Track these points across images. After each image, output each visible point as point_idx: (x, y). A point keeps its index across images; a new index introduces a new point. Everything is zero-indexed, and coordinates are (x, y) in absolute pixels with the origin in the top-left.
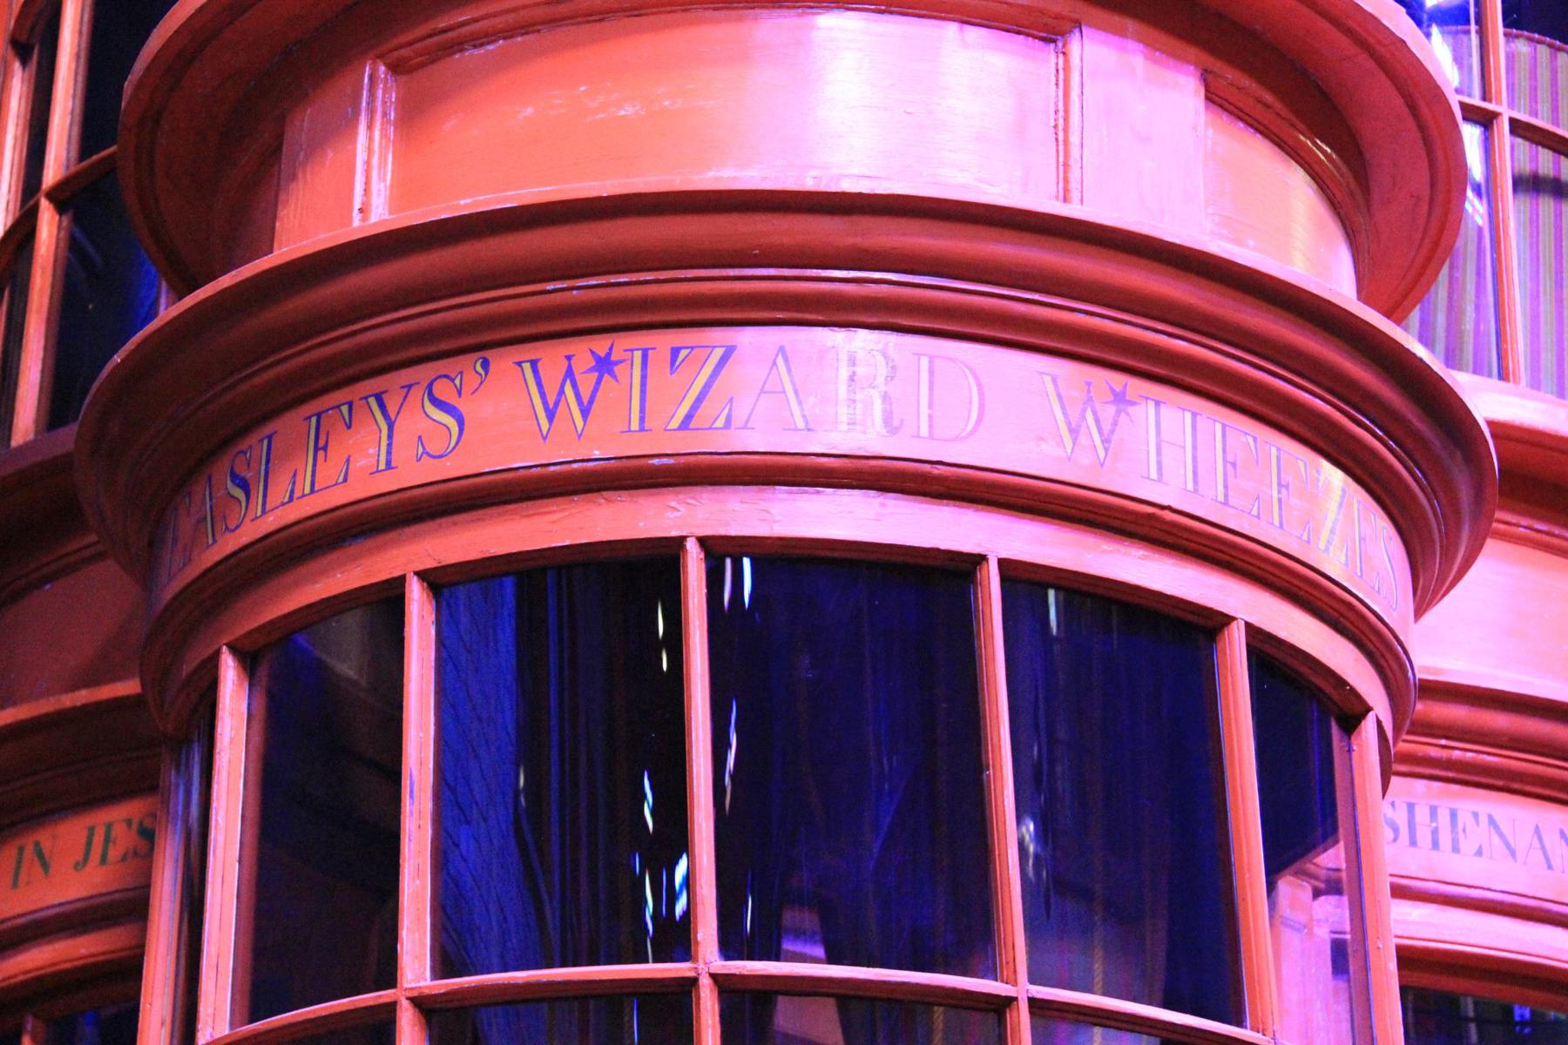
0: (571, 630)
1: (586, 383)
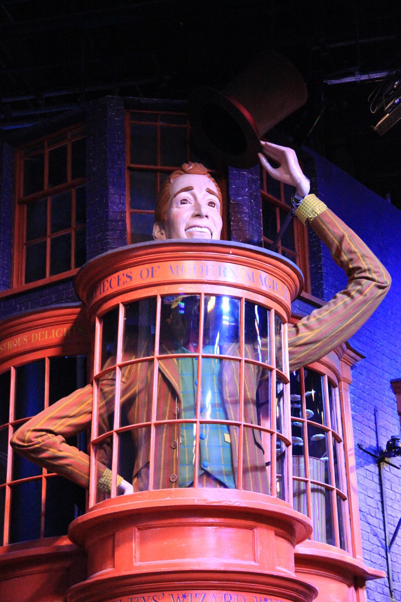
1: (182, 599)
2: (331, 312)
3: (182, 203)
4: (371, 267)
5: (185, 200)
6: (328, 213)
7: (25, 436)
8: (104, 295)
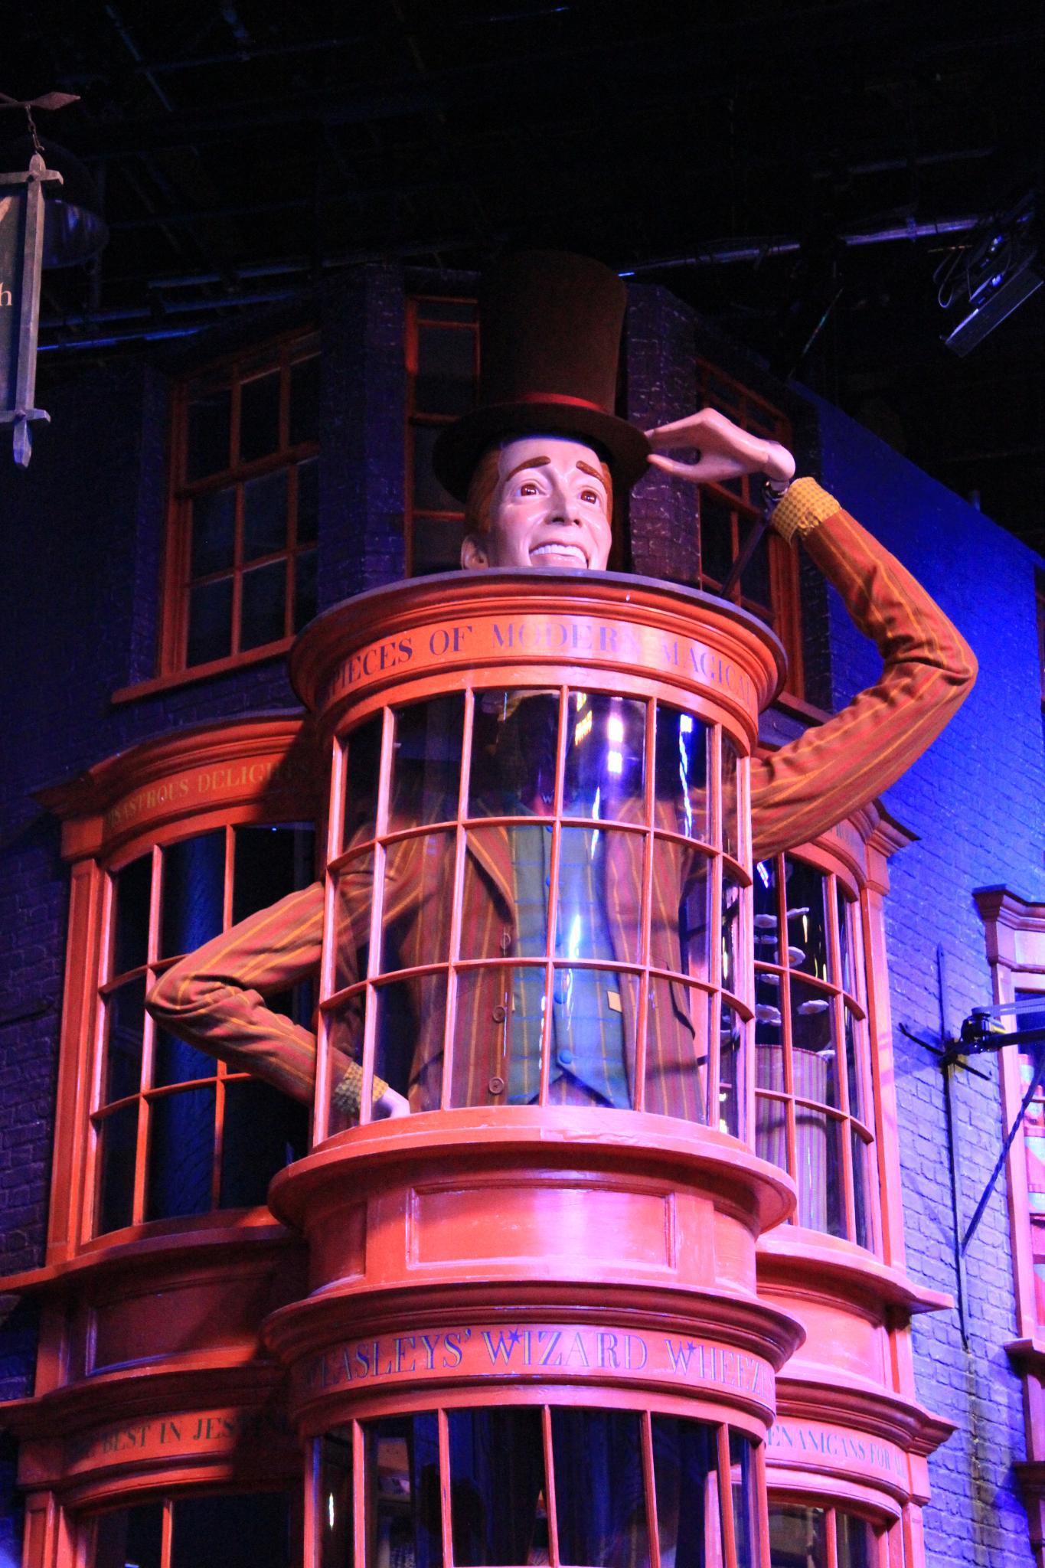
0: (503, 1437)
1: (508, 1342)
2: (846, 732)
3: (524, 493)
4: (934, 636)
5: (532, 486)
6: (842, 518)
7: (177, 989)
8: (350, 688)
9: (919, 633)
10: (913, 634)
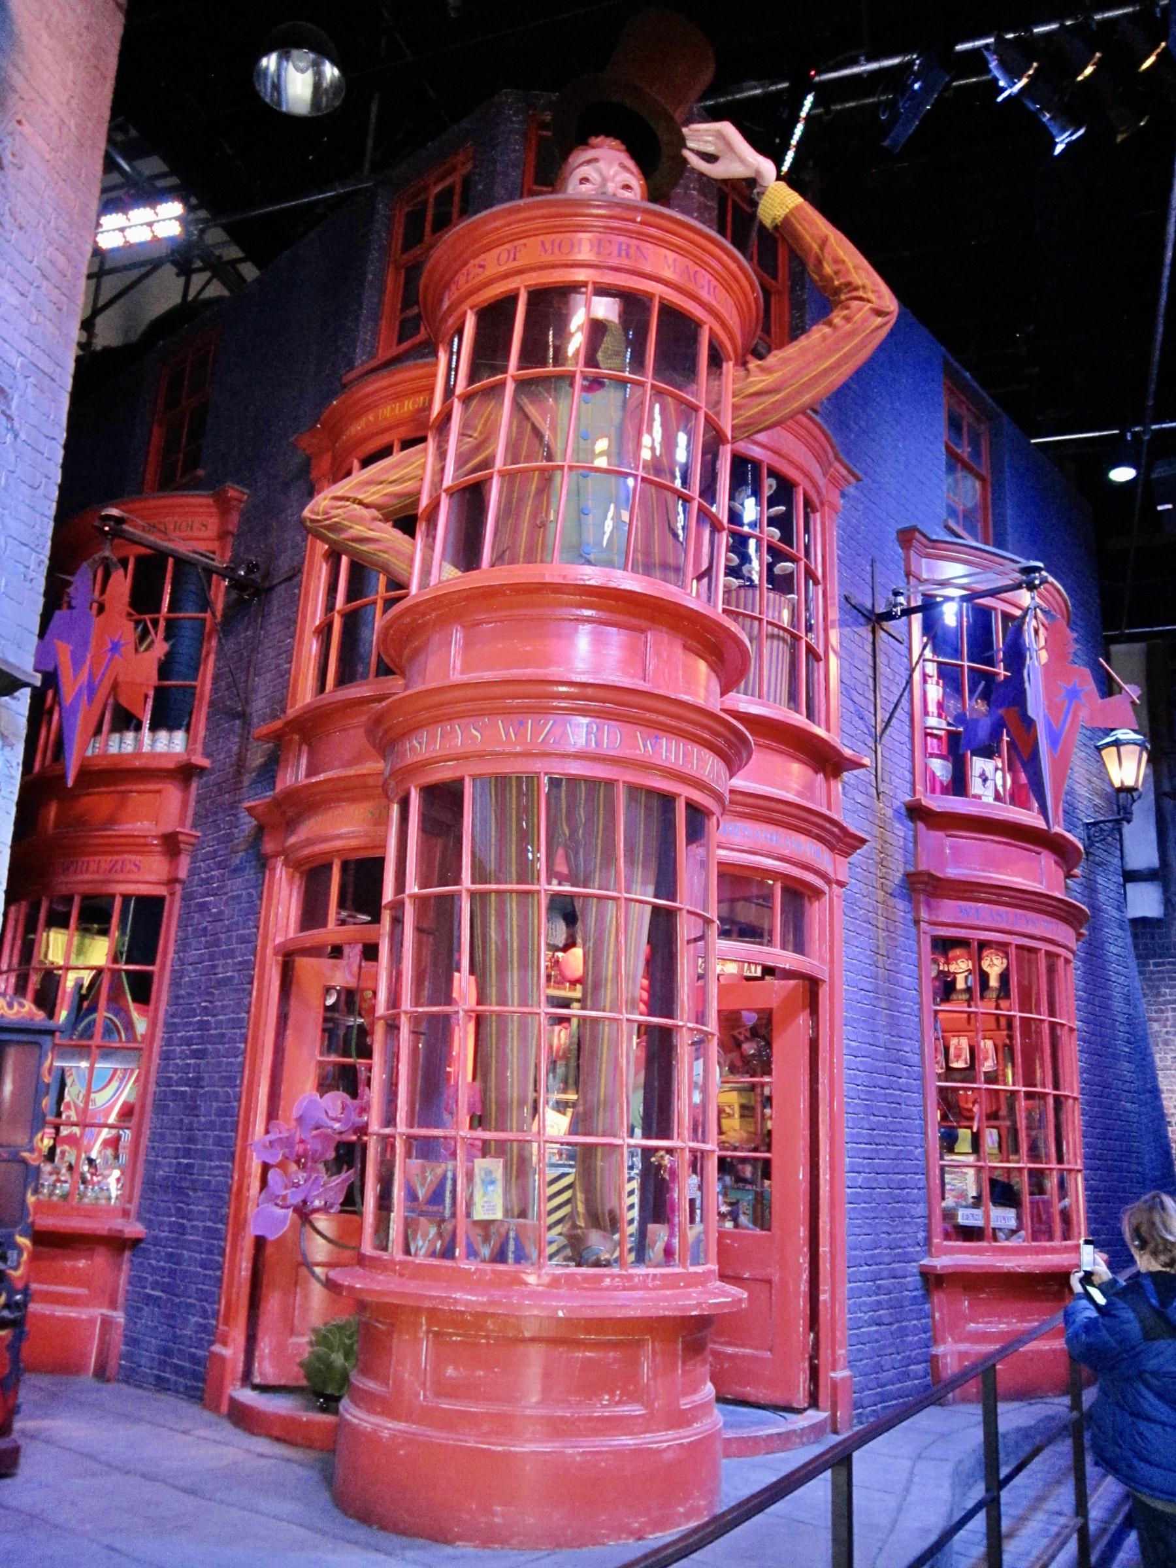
4: (867, 282)
9: (857, 279)
10: (849, 279)
